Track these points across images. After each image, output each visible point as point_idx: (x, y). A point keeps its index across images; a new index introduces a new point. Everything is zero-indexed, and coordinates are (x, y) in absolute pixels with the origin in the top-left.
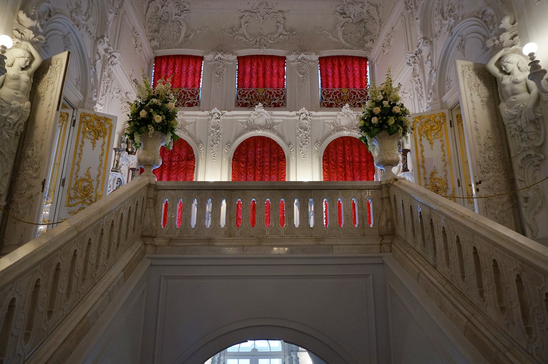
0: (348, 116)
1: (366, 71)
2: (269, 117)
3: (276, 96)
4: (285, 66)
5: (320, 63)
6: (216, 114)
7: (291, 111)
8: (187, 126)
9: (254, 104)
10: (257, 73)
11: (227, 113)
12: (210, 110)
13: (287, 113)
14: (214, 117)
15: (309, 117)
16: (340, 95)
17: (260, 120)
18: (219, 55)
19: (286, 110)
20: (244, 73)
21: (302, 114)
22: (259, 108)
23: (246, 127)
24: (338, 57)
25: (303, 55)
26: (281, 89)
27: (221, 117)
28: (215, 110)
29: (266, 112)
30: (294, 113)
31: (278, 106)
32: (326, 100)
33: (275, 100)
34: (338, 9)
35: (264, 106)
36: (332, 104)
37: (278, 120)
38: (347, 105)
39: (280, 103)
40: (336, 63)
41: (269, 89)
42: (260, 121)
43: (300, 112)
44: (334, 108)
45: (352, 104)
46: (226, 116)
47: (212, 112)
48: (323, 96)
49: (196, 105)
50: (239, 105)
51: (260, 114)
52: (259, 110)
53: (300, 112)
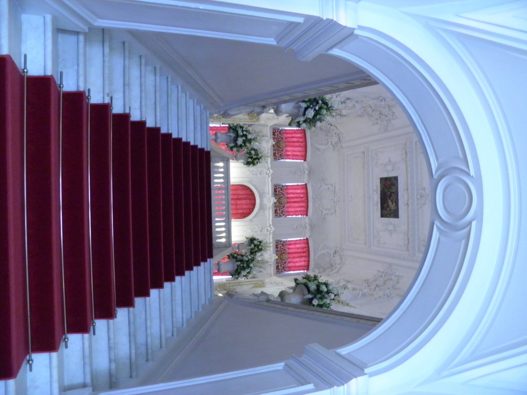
1: (299, 270)
2: (268, 207)
4: (302, 215)
5: (304, 239)
7: (272, 221)
10: (296, 198)
11: (270, 179)
12: (272, 168)
13: (271, 218)
15: (268, 233)
17: (266, 201)
20: (296, 189)
22: (273, 200)
23: (261, 192)
24: (309, 252)
25: (308, 227)
27: (267, 176)
28: (271, 171)
29: (271, 204)
30: (271, 223)
34: (338, 249)
35: (275, 203)
36: (278, 248)
37: (267, 213)
38: (277, 257)
40: (305, 250)
42: (265, 201)
43: (272, 226)
44: (275, 249)
51: (270, 201)
52: (272, 200)
53: (272, 226)
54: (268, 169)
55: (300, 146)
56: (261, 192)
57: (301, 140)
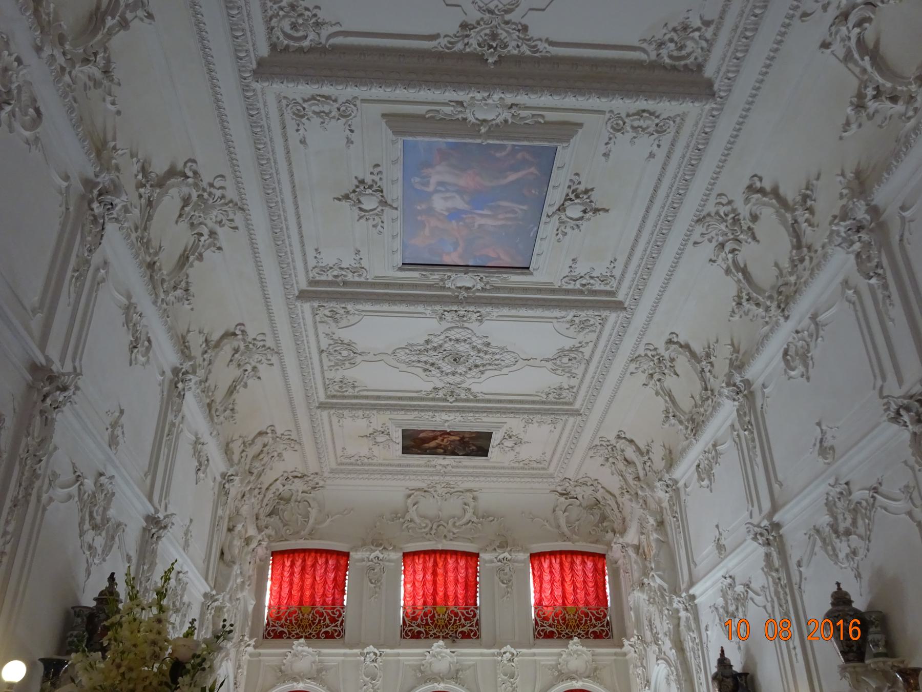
0: (579, 655)
3: (465, 620)
6: (372, 654)
8: (324, 673)
9: (431, 633)
14: (368, 659)
16: (564, 619)
18: (377, 553)
19: (481, 646)
21: (505, 653)
22: (439, 646)
26: (472, 608)
27: (379, 659)
28: (371, 648)
31: (468, 637)
32: (542, 626)
33: (464, 626)
36: (552, 632)
37: (468, 661)
39: (472, 631)
41: (453, 608)
45: (583, 633)
46: (387, 655)
47: (365, 651)
48: (538, 619)
49: (338, 635)
50: (407, 635)
53: (502, 651)
54: (365, 655)
55: (314, 566)
56: (419, 675)
57: (299, 563)
